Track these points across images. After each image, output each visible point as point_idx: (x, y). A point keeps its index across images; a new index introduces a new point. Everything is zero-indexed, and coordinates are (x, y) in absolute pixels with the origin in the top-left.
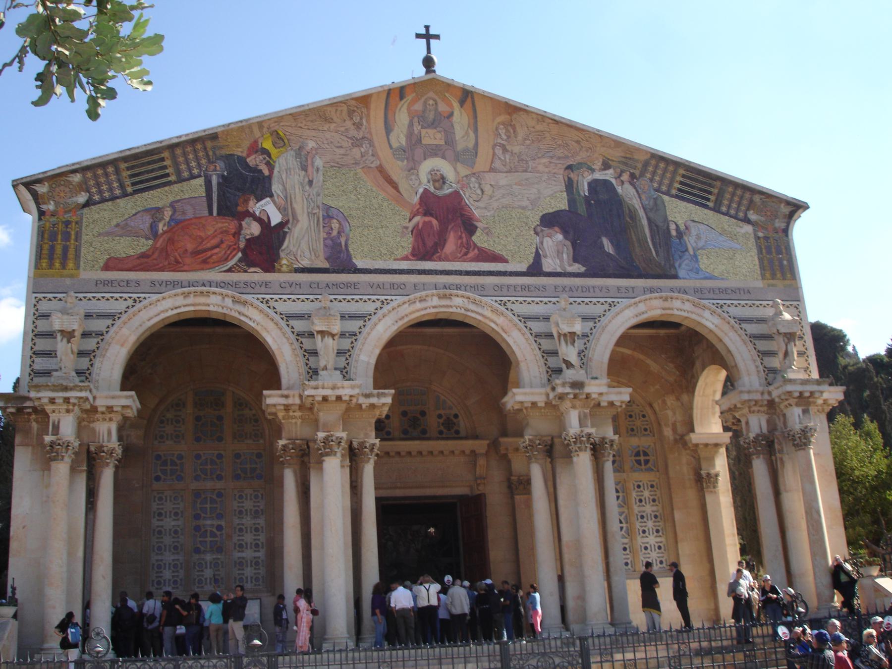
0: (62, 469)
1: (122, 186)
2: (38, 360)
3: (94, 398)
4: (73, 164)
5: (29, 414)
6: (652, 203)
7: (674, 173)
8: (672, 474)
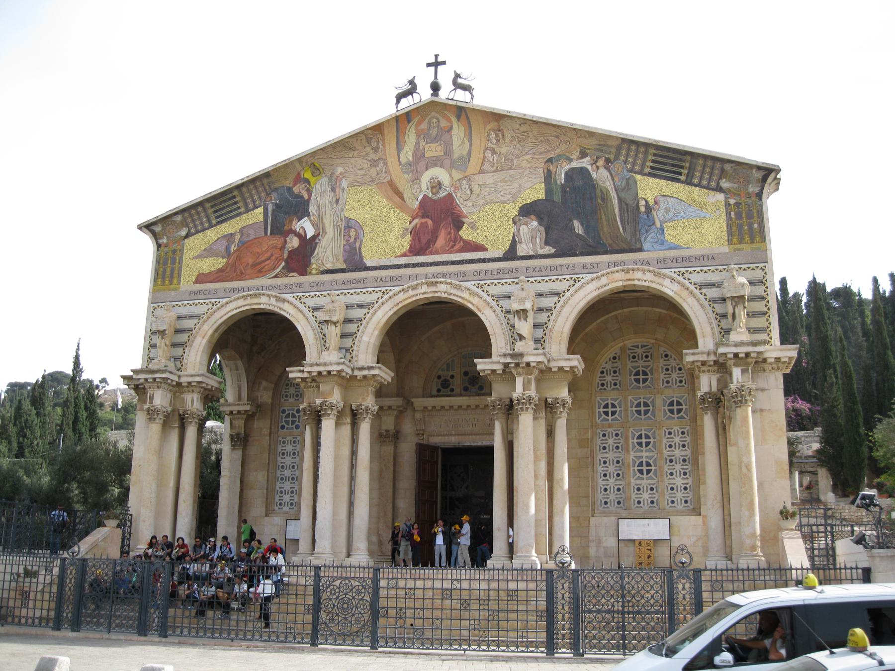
0: (156, 428)
1: (209, 221)
2: (152, 351)
3: (179, 377)
7: (646, 153)
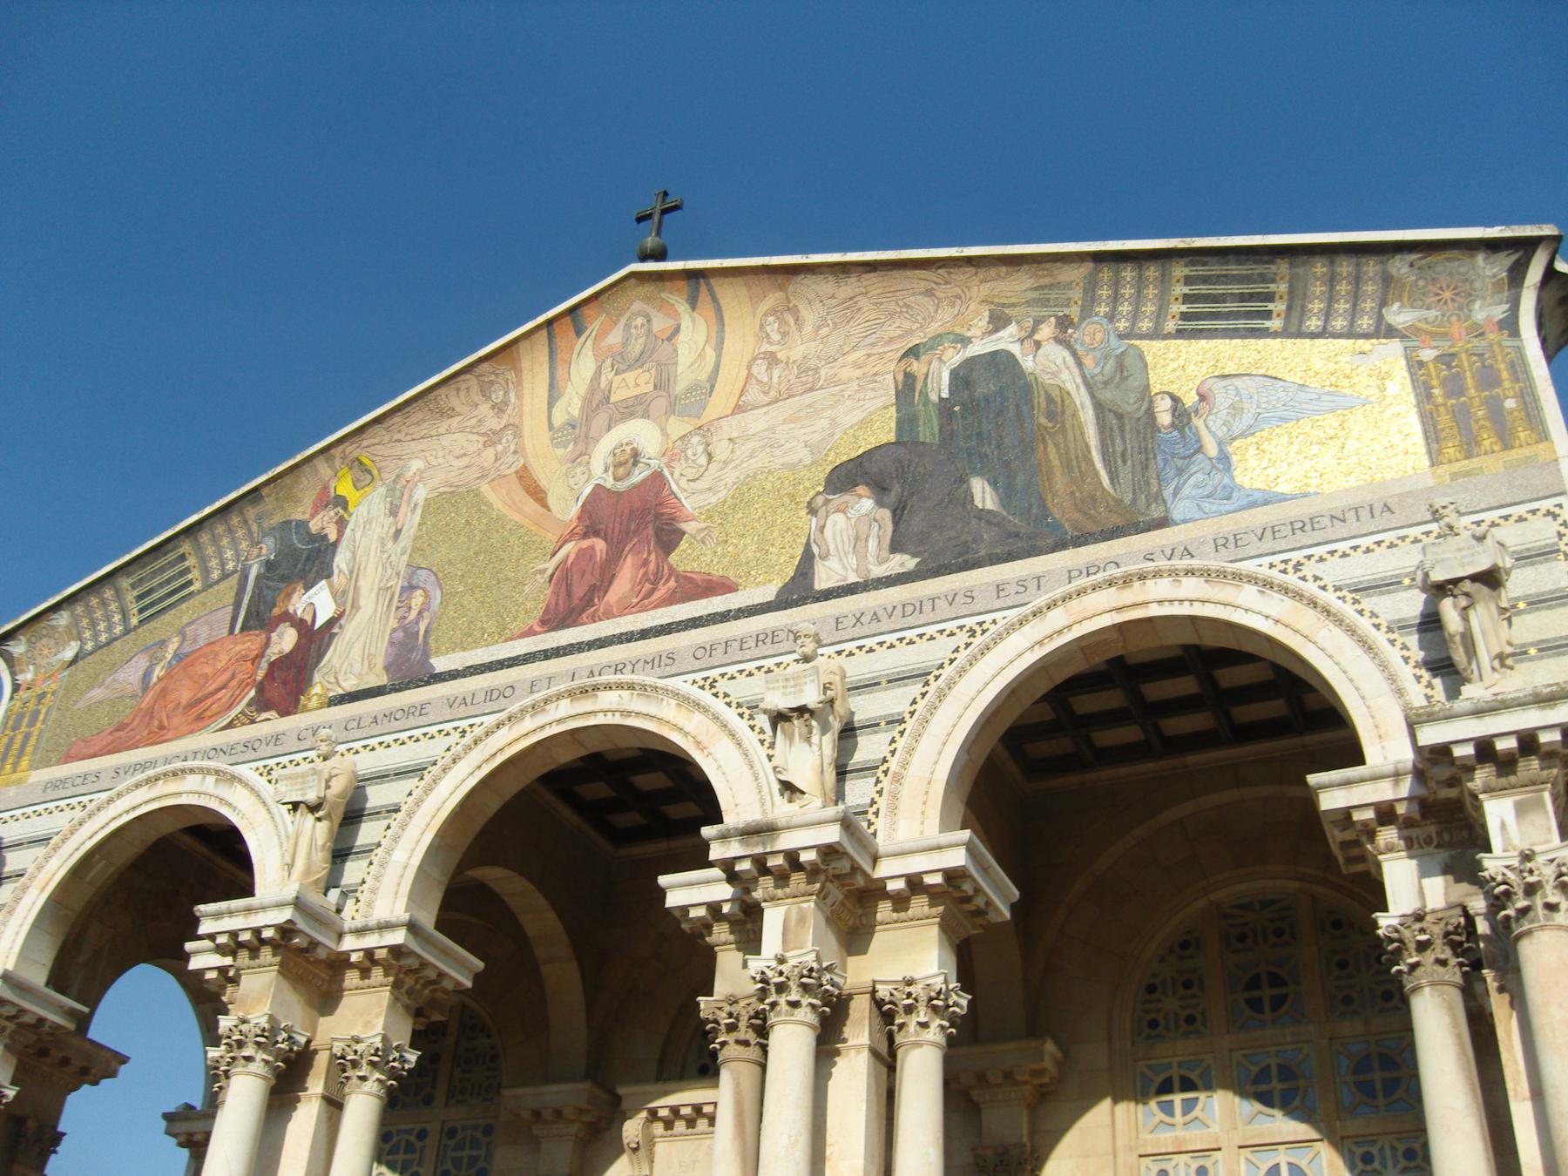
6: (1110, 365)
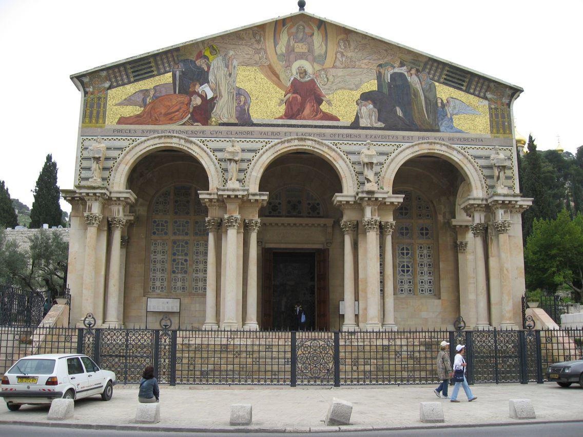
0: (92, 230)
2: (83, 172)
3: (110, 193)
4: (102, 66)
5: (77, 200)
6: (428, 85)
7: (443, 69)
8: (440, 242)
